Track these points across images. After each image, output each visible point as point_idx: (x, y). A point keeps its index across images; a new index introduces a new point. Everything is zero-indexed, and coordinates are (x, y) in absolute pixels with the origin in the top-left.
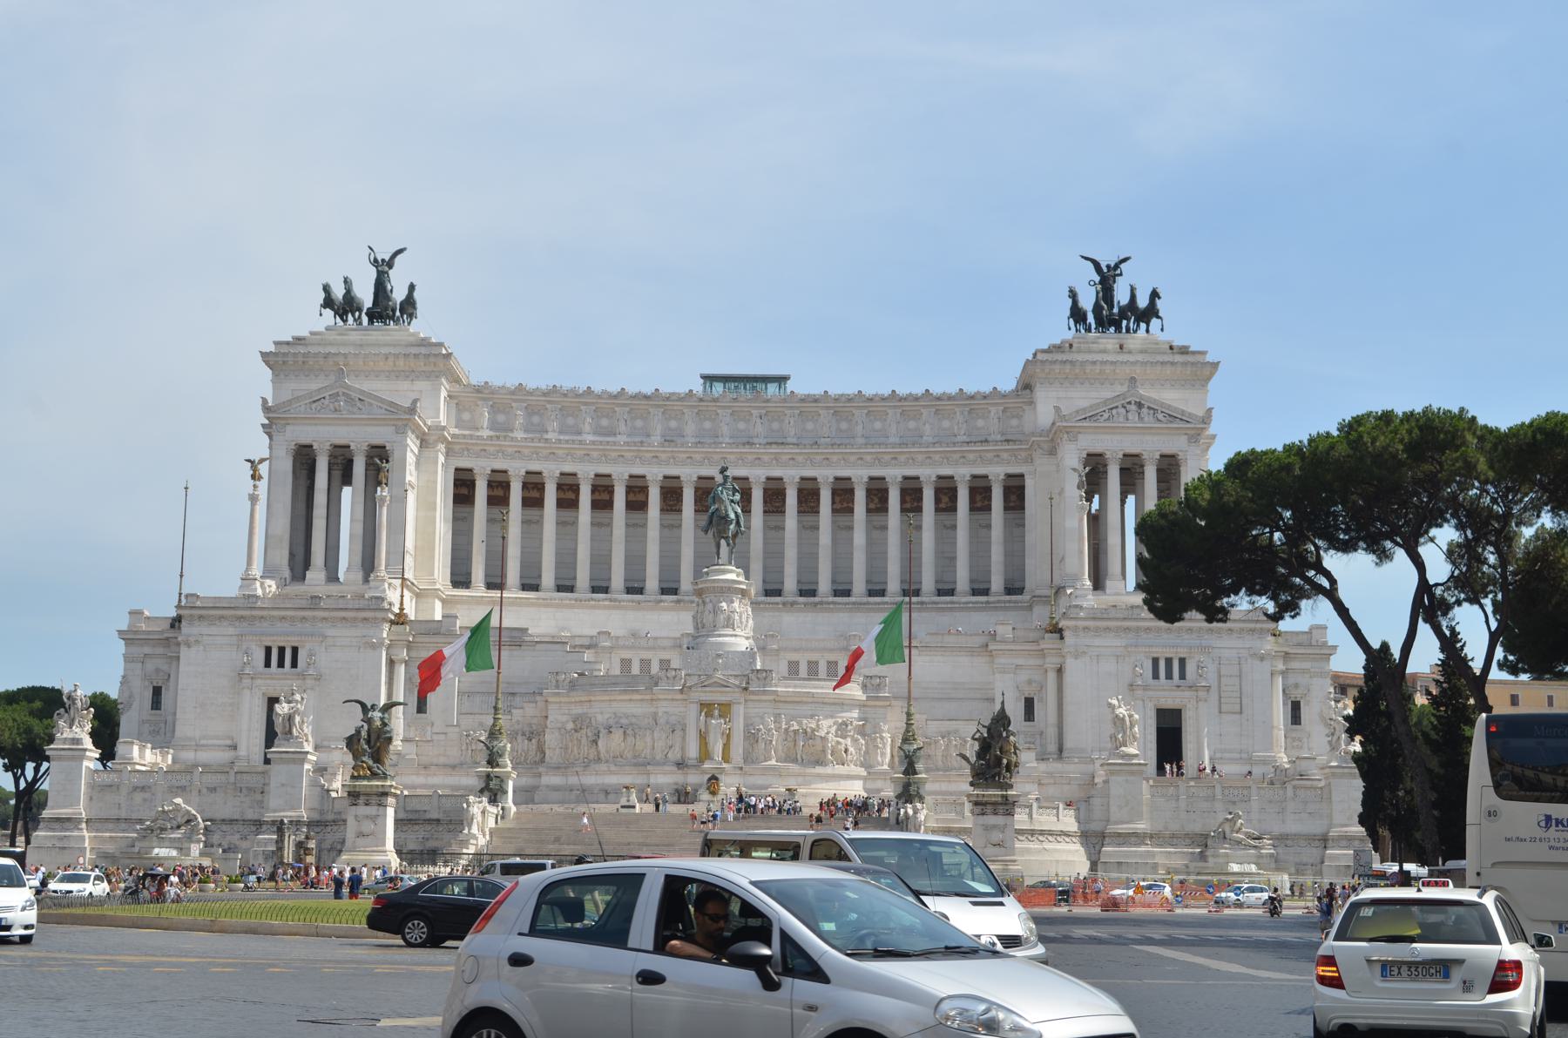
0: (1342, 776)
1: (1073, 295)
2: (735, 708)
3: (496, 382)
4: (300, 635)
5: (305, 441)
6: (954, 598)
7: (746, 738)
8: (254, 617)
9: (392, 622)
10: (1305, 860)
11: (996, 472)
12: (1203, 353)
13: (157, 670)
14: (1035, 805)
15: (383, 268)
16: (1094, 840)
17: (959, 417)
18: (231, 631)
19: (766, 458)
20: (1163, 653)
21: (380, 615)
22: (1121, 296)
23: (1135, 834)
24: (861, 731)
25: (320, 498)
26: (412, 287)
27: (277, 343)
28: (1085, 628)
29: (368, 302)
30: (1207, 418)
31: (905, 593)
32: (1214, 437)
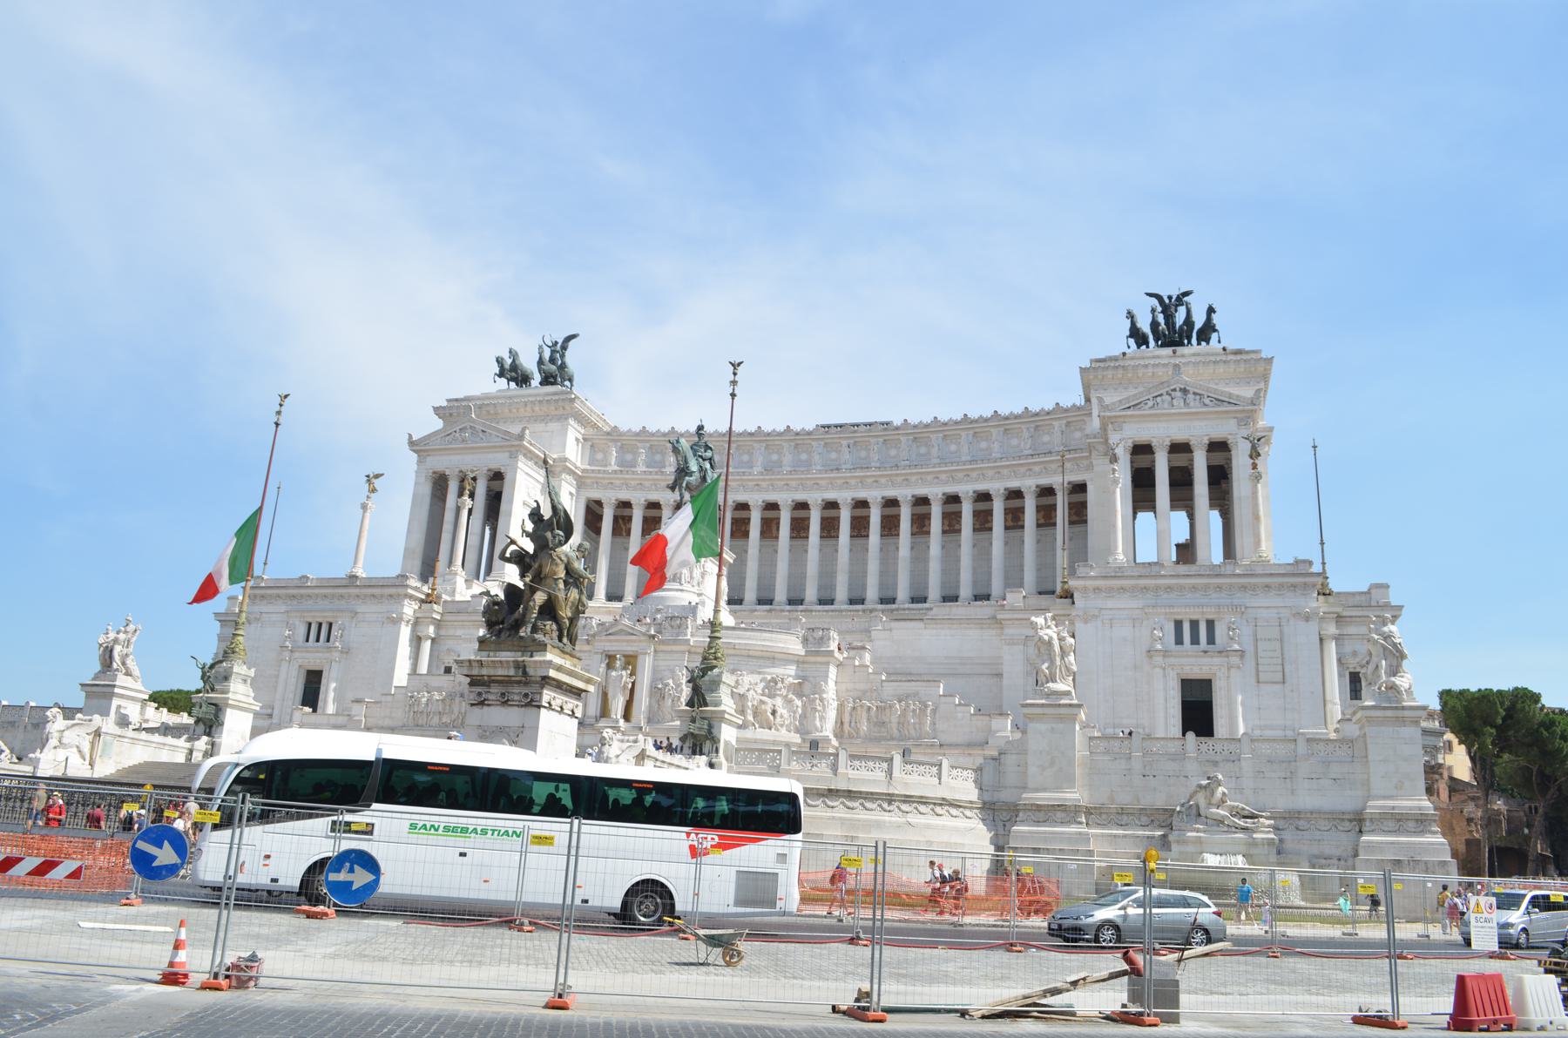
0: (1383, 722)
1: (1131, 316)
3: (624, 428)
4: (332, 610)
5: (440, 468)
9: (422, 601)
10: (1327, 851)
14: (897, 759)
16: (1005, 816)
17: (1026, 434)
18: (283, 608)
19: (853, 482)
20: (1186, 615)
21: (401, 591)
23: (1061, 807)
24: (798, 690)
25: (449, 516)
28: (1097, 589)
32: (1271, 429)
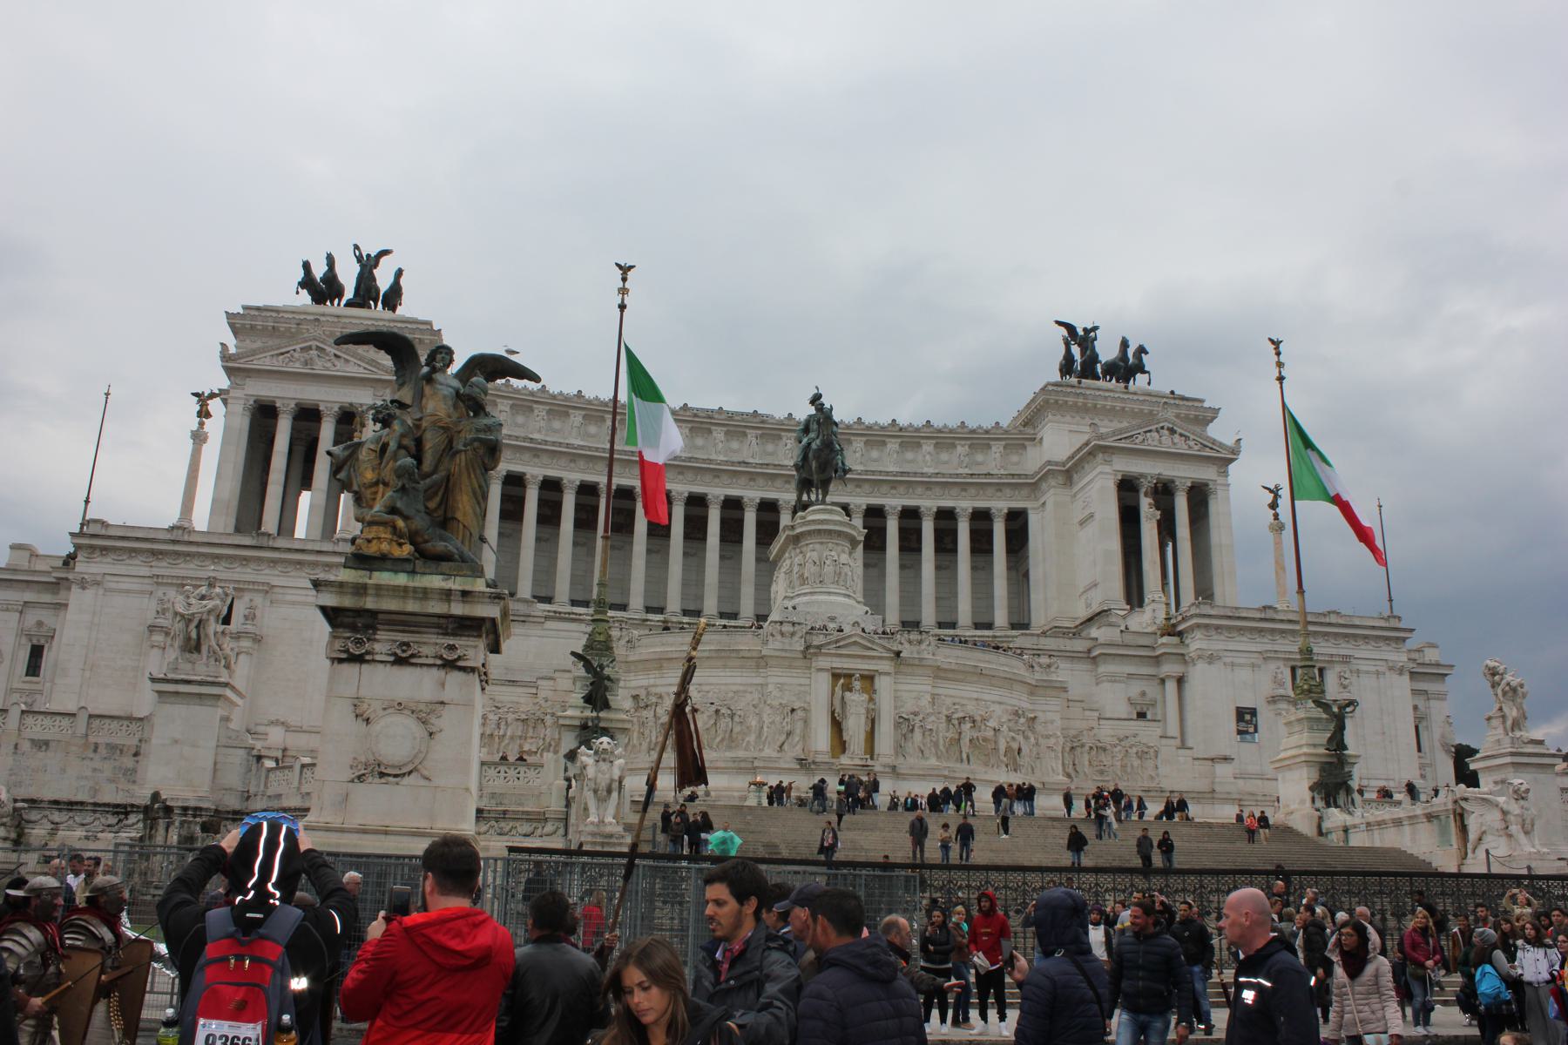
2: (882, 684)
6: (958, 632)
7: (897, 725)
8: (177, 554)
11: (1000, 505)
12: (1202, 401)
13: (40, 624)
15: (368, 265)
18: (145, 571)
22: (1107, 351)
26: (399, 273)
27: (245, 308)
28: (1217, 628)
29: (349, 294)
30: (1235, 451)
31: (904, 624)
